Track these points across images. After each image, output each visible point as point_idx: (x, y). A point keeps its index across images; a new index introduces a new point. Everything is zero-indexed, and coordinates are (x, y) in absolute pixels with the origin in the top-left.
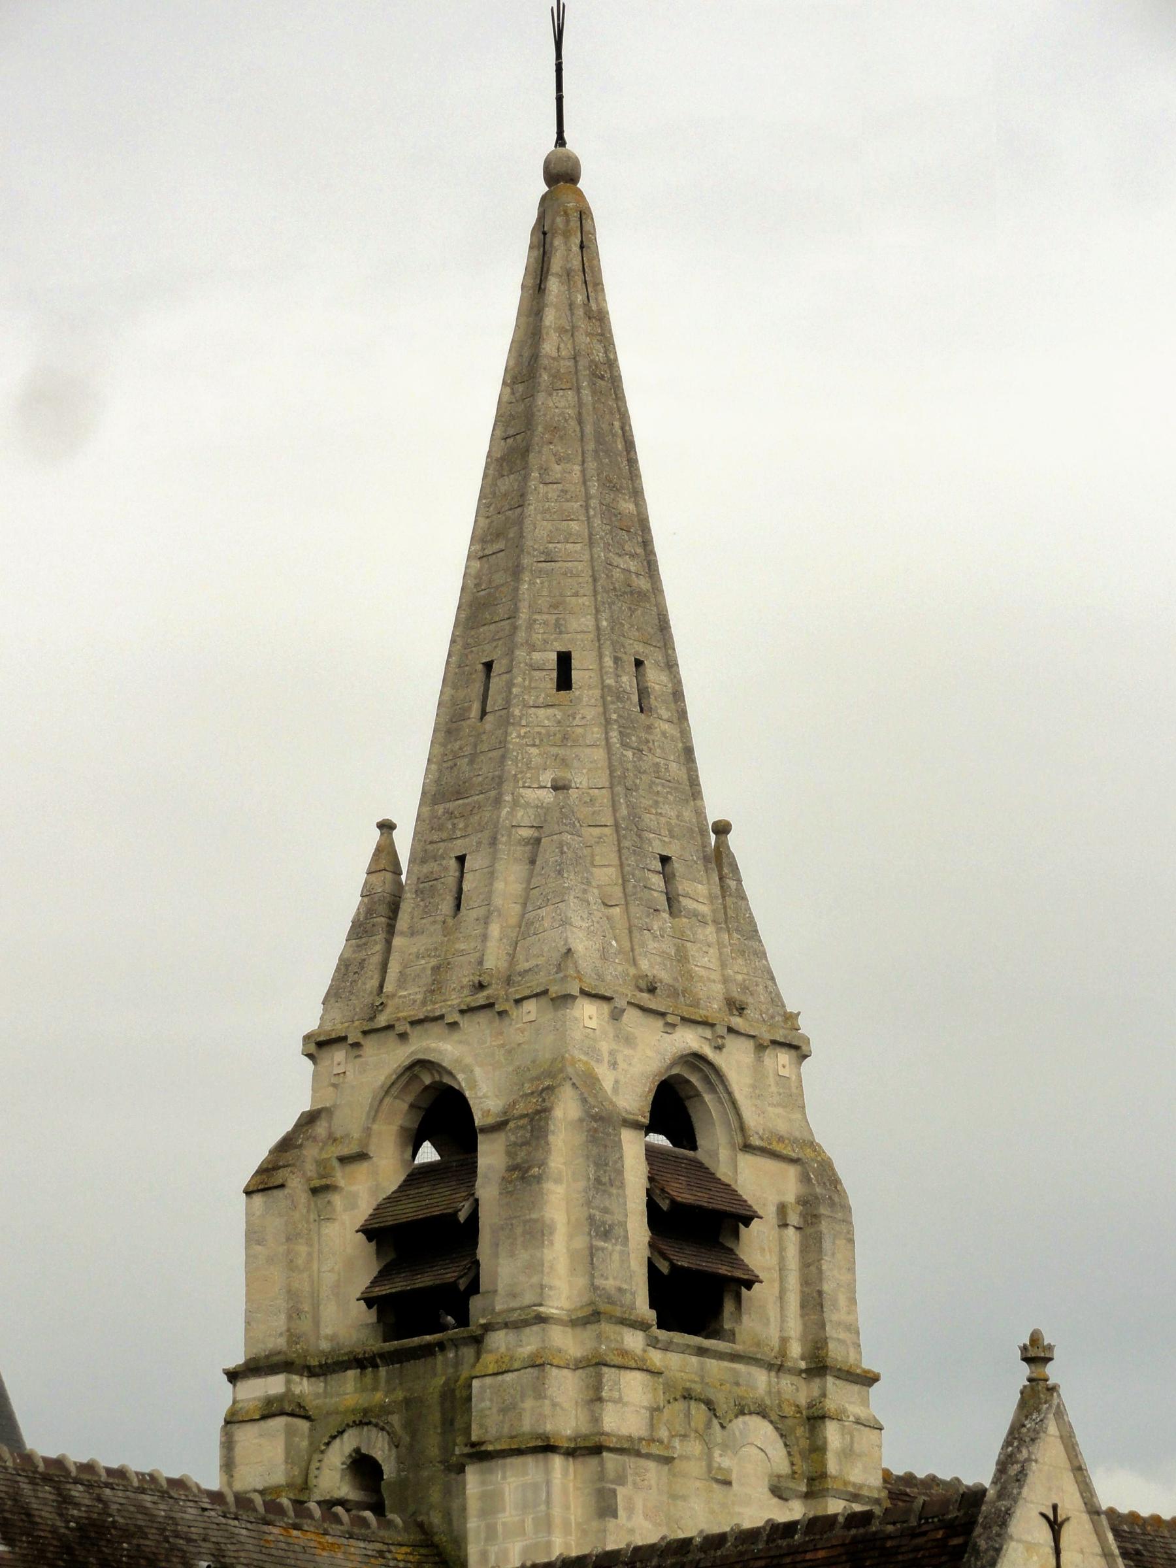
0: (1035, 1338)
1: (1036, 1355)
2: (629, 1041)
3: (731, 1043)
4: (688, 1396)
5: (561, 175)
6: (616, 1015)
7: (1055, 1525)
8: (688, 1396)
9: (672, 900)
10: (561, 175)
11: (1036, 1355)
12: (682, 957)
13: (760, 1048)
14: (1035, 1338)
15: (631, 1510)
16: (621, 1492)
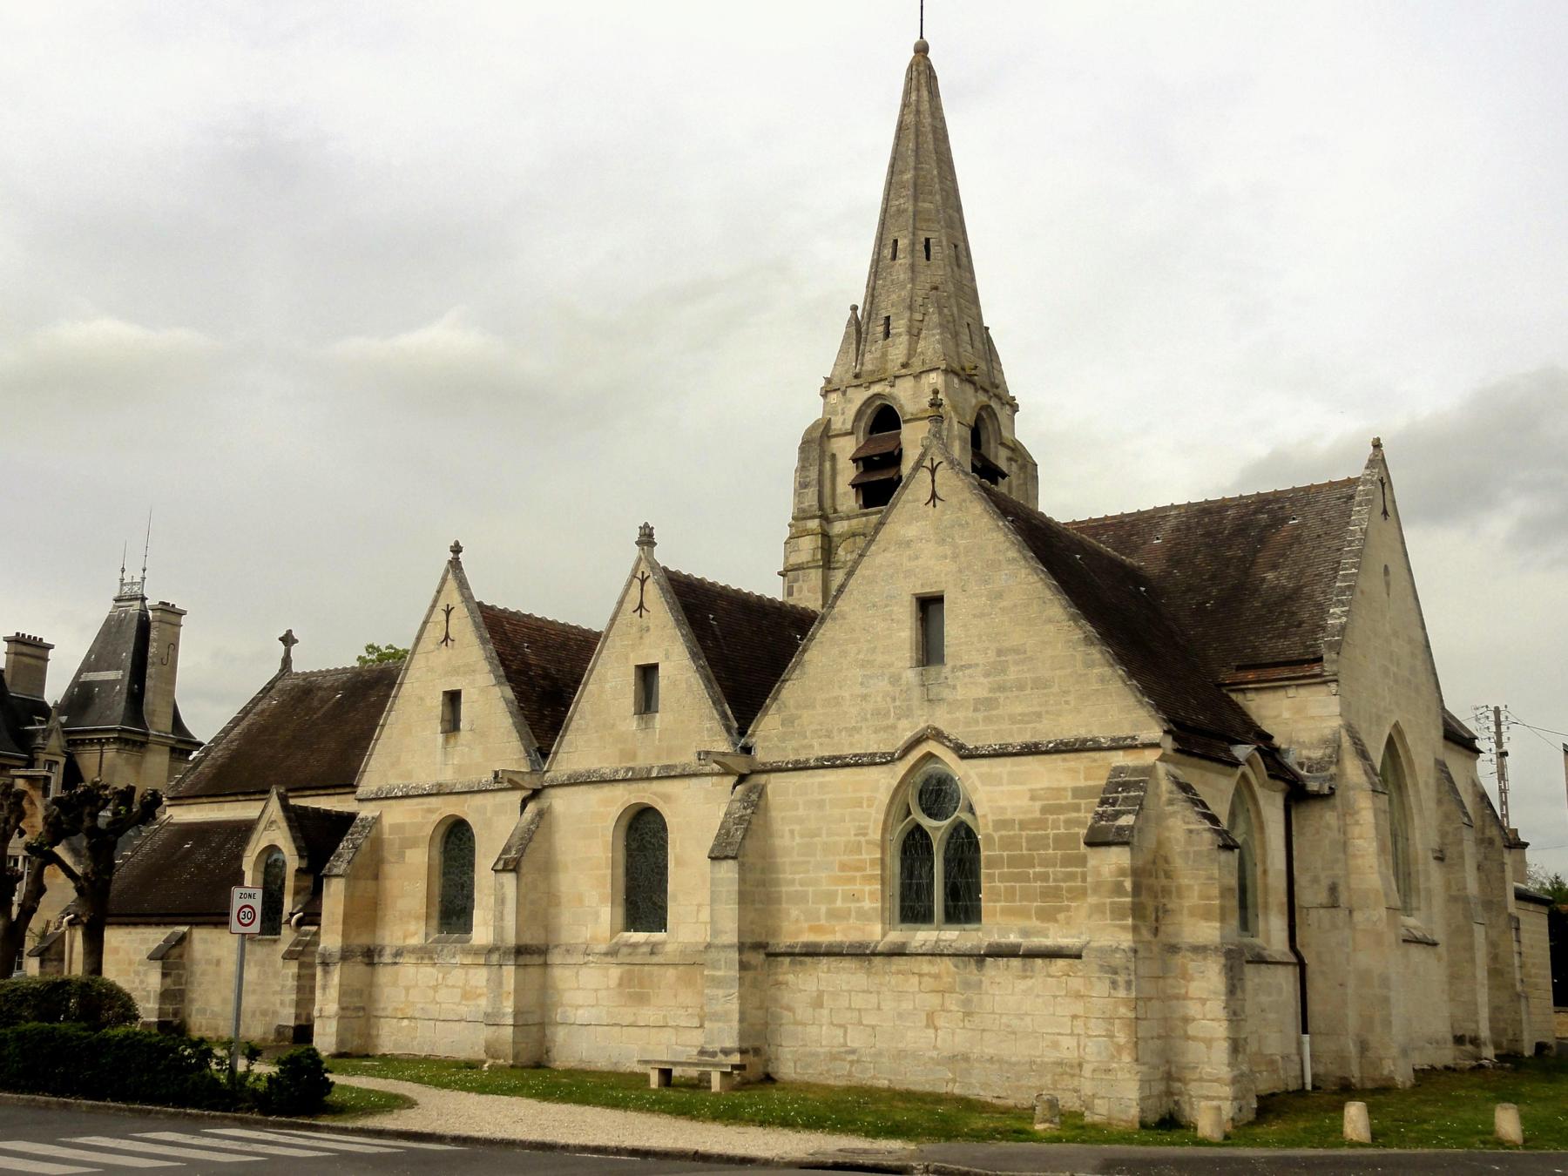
0: (457, 544)
1: (457, 549)
2: (850, 401)
3: (898, 382)
4: (854, 535)
5: (922, 49)
6: (844, 393)
7: (448, 613)
8: (854, 535)
9: (887, 334)
10: (922, 49)
11: (457, 549)
12: (884, 354)
13: (917, 376)
14: (457, 544)
15: (800, 591)
16: (796, 586)
